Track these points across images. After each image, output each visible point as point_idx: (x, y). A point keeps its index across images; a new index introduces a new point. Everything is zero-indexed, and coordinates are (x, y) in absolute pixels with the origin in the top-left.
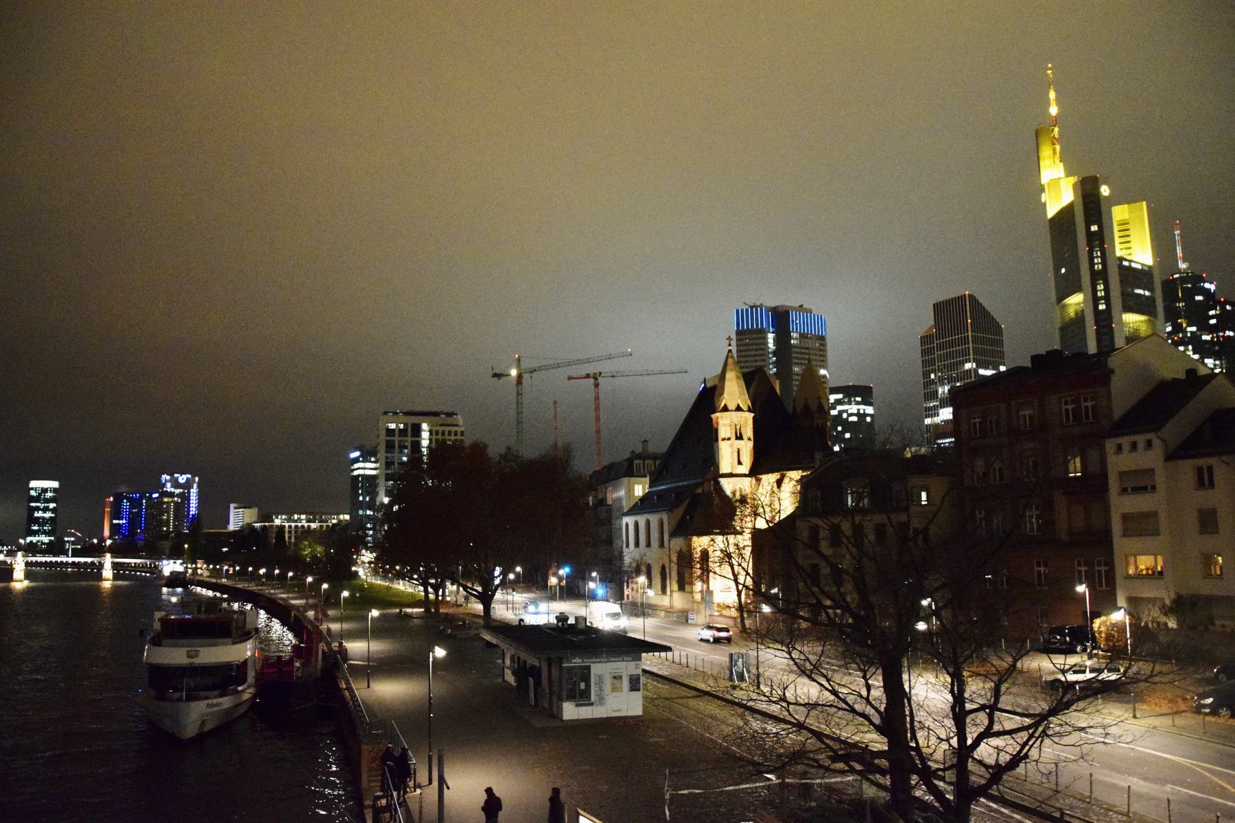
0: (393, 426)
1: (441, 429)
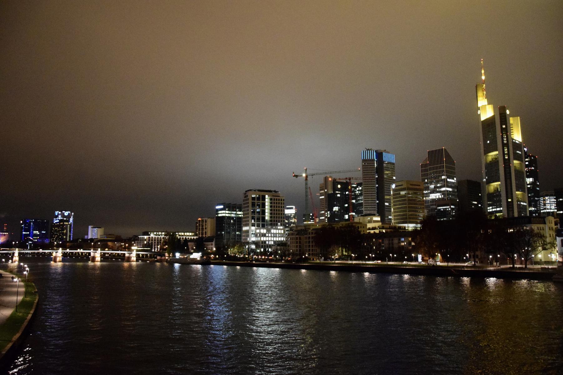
0: (253, 196)
1: (273, 198)
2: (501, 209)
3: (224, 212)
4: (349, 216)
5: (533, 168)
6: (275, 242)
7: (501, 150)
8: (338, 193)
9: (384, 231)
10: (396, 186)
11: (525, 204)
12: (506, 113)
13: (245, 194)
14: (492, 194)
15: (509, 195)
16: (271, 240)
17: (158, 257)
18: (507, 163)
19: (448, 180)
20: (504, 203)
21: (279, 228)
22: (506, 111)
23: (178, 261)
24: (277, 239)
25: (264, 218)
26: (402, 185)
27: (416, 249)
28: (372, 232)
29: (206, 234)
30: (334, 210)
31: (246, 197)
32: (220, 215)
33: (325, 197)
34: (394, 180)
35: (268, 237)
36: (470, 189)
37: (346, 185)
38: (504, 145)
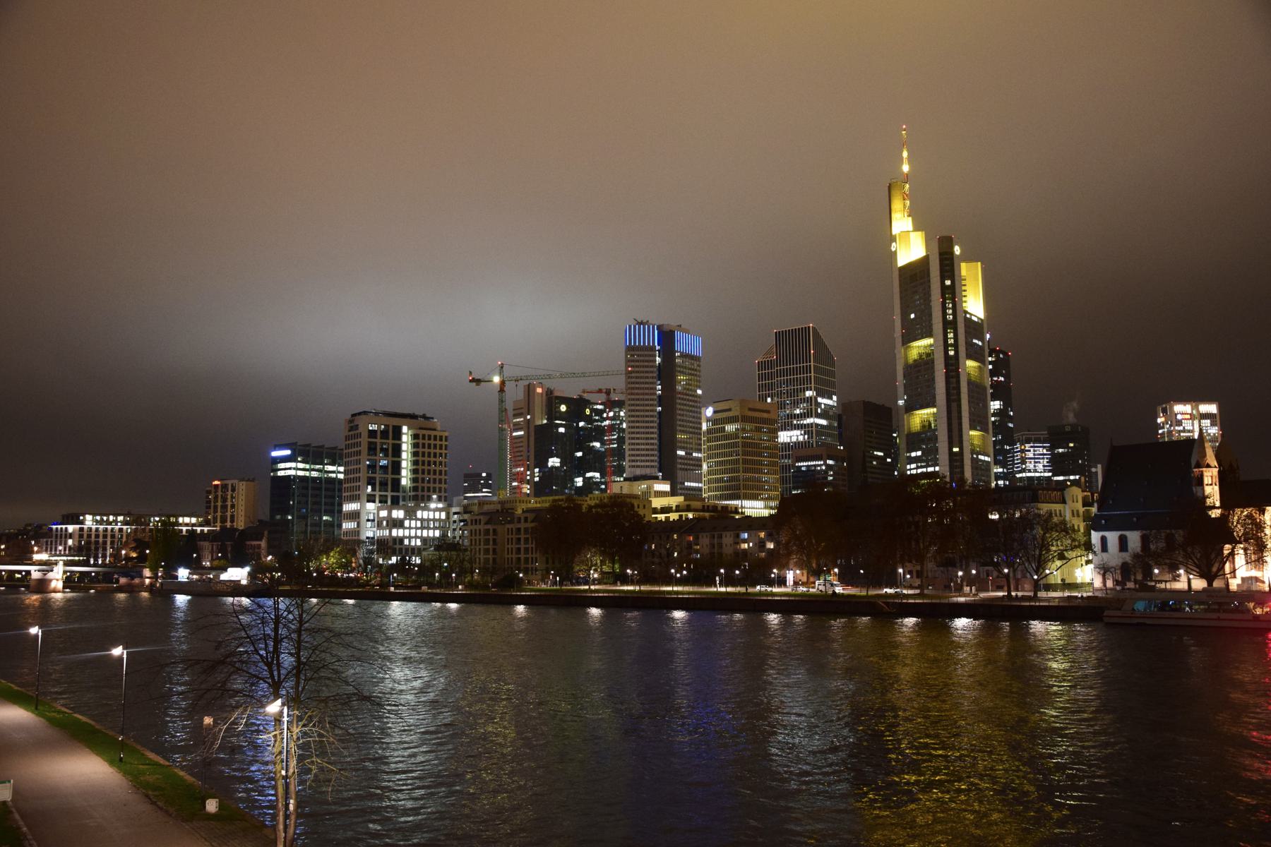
0: (375, 427)
1: (421, 432)
2: (937, 469)
3: (293, 465)
4: (586, 480)
5: (1002, 379)
6: (424, 540)
7: (941, 337)
8: (561, 425)
9: (690, 516)
10: (715, 412)
11: (987, 459)
12: (952, 253)
13: (351, 421)
14: (918, 434)
15: (956, 439)
16: (416, 537)
17: (123, 580)
18: (952, 366)
19: (820, 400)
20: (943, 456)
21: (433, 506)
22: (952, 248)
23: (183, 588)
24: (431, 534)
25: (399, 481)
26: (730, 410)
27: (780, 559)
28: (662, 517)
29: (232, 521)
30: (550, 464)
31: (351, 429)
32: (280, 473)
33: (528, 433)
34: (699, 396)
35: (410, 528)
36: (867, 423)
37: (578, 406)
38: (947, 325)
